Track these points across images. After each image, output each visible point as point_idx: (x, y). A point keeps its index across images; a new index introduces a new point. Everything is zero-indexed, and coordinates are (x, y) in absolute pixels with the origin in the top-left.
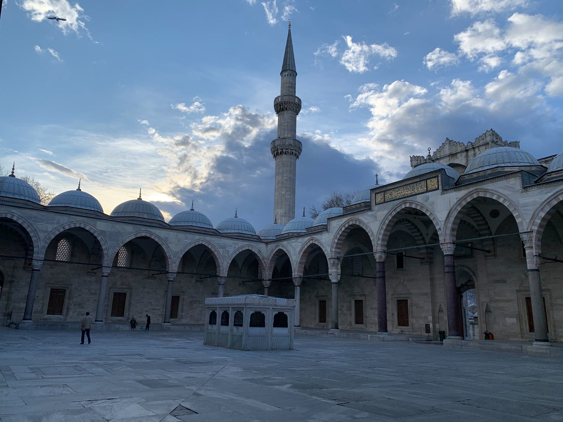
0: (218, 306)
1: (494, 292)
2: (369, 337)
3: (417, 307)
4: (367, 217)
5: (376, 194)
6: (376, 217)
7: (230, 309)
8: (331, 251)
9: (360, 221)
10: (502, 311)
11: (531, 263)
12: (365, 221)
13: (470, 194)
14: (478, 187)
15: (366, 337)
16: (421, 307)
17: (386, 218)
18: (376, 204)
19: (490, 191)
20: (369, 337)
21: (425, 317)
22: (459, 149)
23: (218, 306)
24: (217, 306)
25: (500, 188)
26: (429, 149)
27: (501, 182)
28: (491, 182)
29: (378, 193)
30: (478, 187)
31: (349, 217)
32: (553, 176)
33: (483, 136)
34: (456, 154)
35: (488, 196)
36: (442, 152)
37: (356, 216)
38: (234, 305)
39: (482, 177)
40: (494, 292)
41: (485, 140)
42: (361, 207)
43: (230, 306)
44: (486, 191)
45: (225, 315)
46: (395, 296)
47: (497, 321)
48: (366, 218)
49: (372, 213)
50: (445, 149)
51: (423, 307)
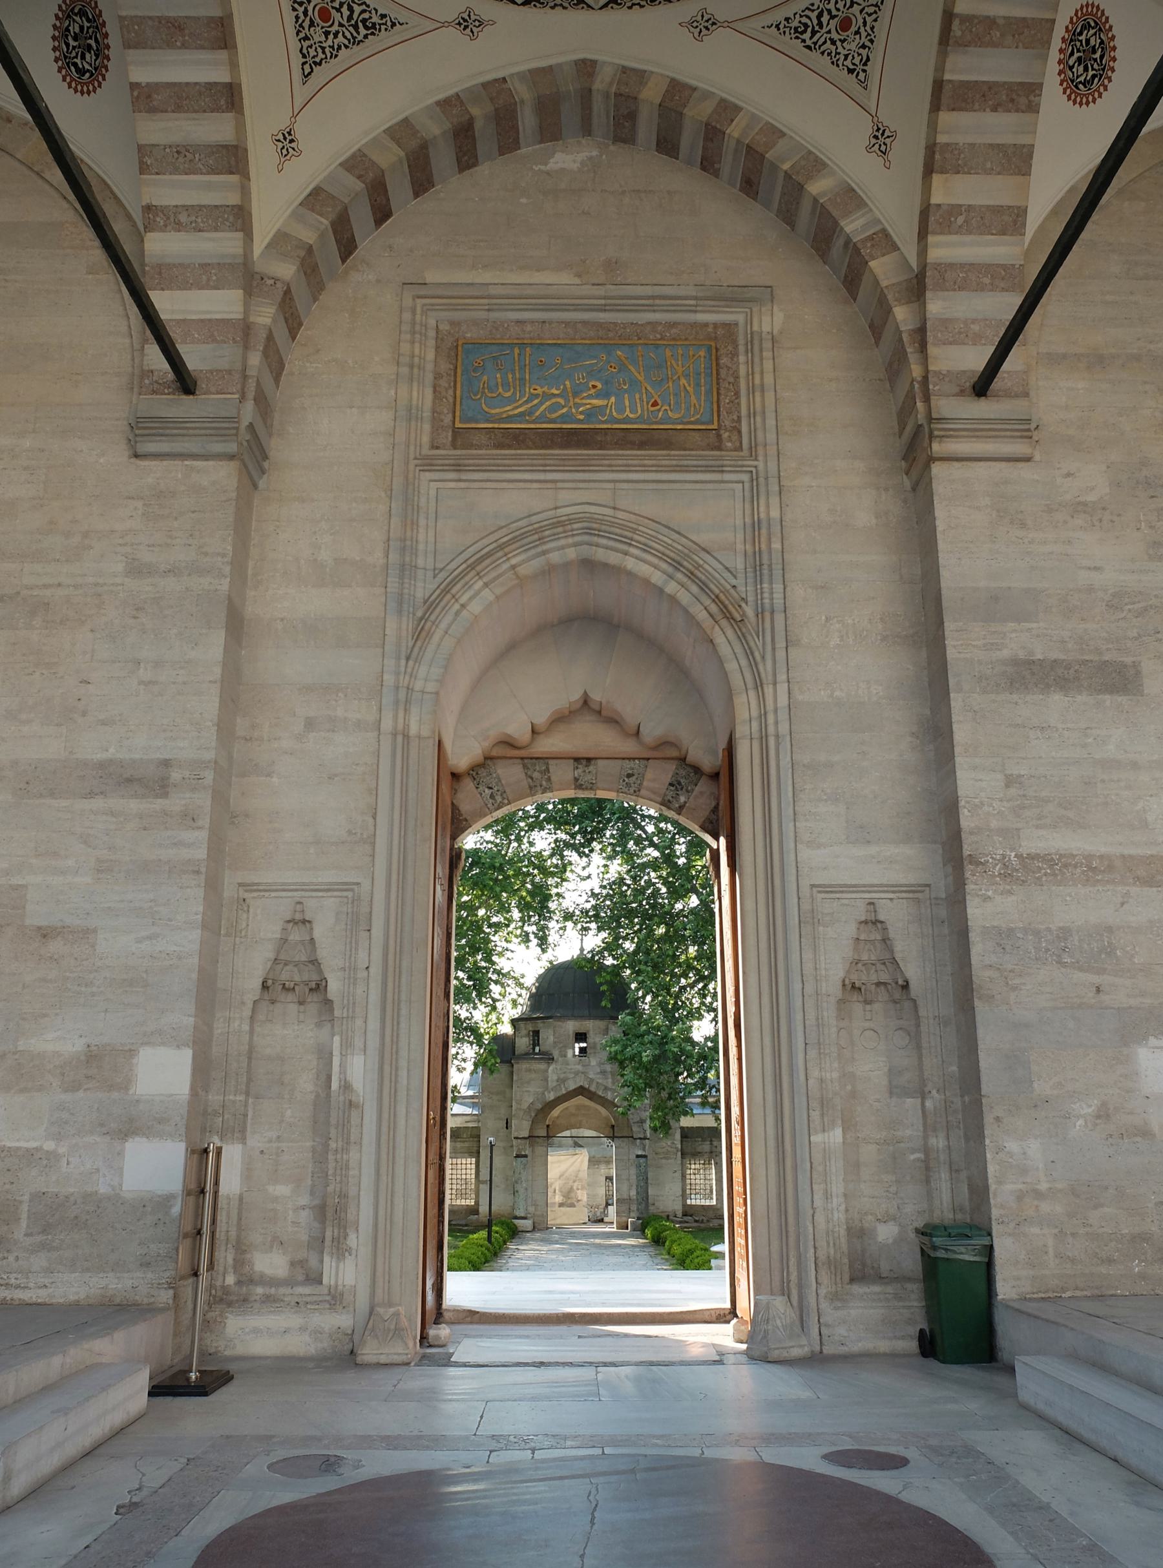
1: (1010, 781)
16: (45, 934)
21: (92, 1057)
40: (1010, 781)
47: (1042, 1087)
51: (87, 934)
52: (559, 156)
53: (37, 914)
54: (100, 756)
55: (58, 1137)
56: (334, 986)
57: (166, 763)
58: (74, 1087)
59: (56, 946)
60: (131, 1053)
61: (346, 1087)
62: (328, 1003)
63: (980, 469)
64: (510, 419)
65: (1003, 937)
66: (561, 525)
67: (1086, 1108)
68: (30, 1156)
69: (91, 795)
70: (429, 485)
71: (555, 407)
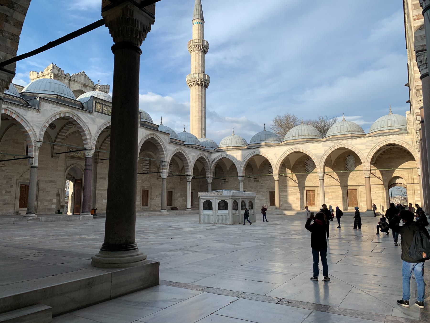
0: (240, 198)
1: (99, 184)
2: (81, 218)
3: (43, 192)
4: (87, 118)
5: (96, 102)
6: (95, 122)
7: (214, 199)
8: (40, 134)
9: (79, 118)
10: (101, 196)
11: (165, 175)
12: (85, 121)
13: (150, 135)
14: (155, 133)
15: (78, 218)
16: (47, 192)
17: (102, 126)
18: (95, 111)
19: (158, 137)
20: (81, 218)
21: (50, 200)
22: (91, 85)
23: (248, 198)
24: (239, 197)
25: (162, 138)
26: (99, 81)
27: (162, 135)
28: (160, 133)
29: (98, 103)
30: (155, 133)
31: (68, 109)
32: (174, 141)
33: (105, 86)
34: (87, 86)
35: (157, 139)
36: (79, 78)
37: (76, 112)
38: (250, 197)
39: (149, 126)
40: (99, 184)
41: (105, 89)
42: (76, 105)
43: (248, 198)
44: (157, 136)
45: (243, 203)
46: (20, 181)
47: (98, 202)
48: (86, 118)
49: (91, 117)
50: (81, 78)
52: (76, 134)
53: (47, 190)
54: (50, 180)
55: (48, 205)
56: (60, 195)
57: (54, 181)
58: (49, 201)
59: (48, 193)
60: (52, 199)
61: (61, 201)
62: (60, 196)
63: (100, 165)
64: (72, 155)
65: (98, 193)
66: (75, 164)
67: (100, 203)
68: (47, 206)
69: (50, 183)
70: (66, 159)
71: (74, 155)
